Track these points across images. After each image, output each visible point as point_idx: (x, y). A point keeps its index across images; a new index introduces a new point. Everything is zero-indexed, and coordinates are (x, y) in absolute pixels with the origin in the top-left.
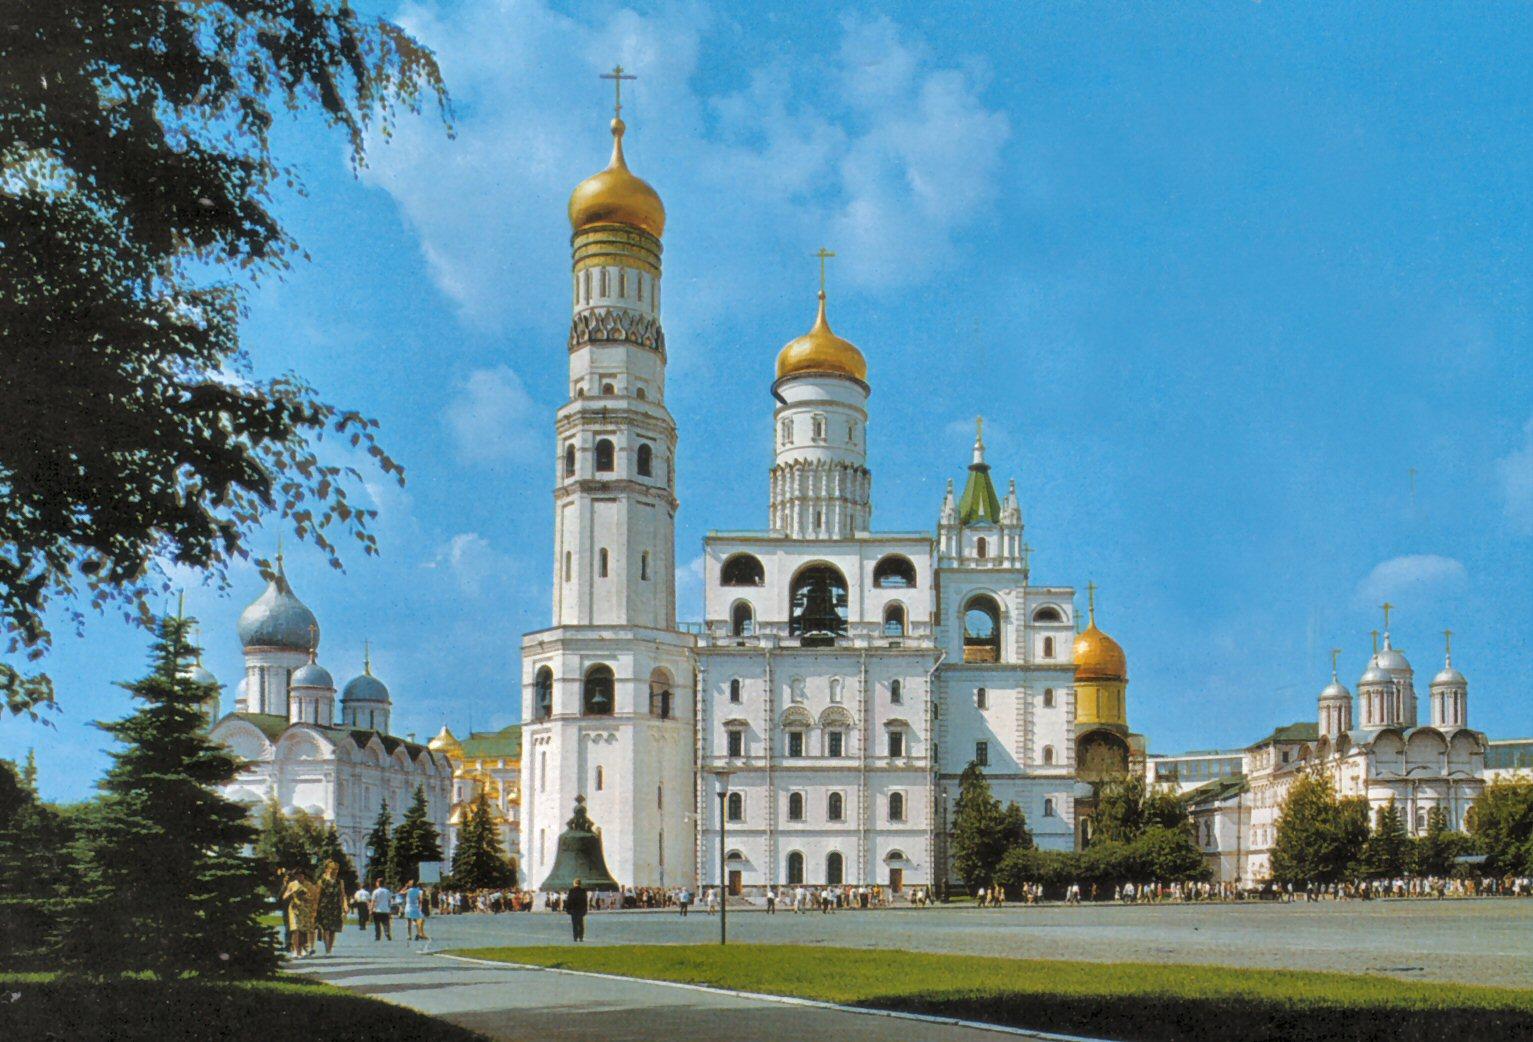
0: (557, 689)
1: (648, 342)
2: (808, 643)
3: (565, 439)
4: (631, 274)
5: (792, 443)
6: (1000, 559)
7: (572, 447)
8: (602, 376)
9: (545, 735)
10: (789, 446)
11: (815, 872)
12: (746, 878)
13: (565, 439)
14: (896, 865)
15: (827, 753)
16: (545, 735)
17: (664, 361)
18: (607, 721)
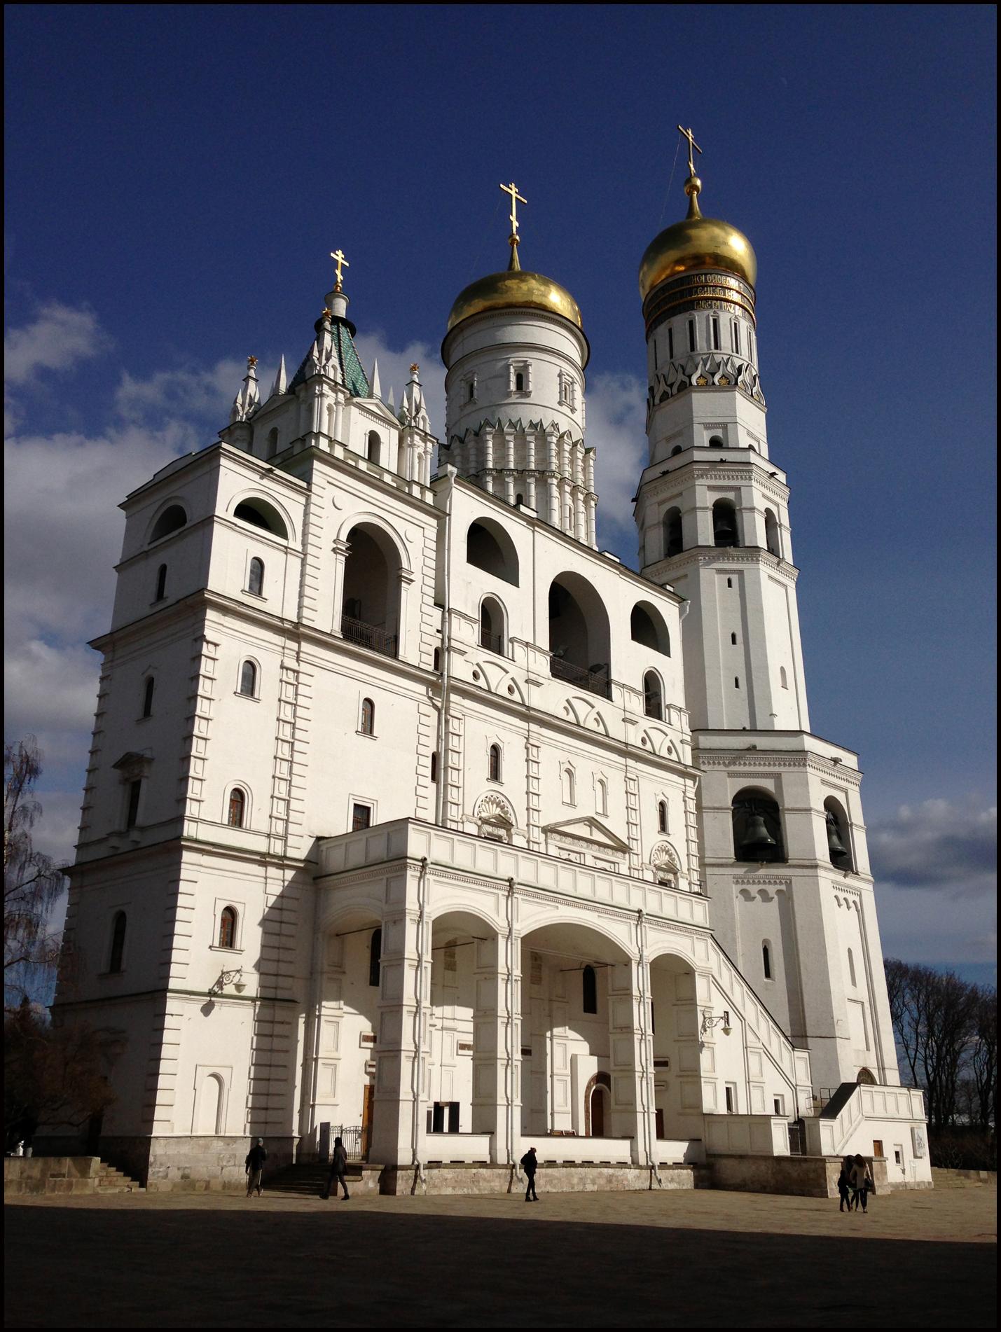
8: (708, 426)
13: (660, 503)
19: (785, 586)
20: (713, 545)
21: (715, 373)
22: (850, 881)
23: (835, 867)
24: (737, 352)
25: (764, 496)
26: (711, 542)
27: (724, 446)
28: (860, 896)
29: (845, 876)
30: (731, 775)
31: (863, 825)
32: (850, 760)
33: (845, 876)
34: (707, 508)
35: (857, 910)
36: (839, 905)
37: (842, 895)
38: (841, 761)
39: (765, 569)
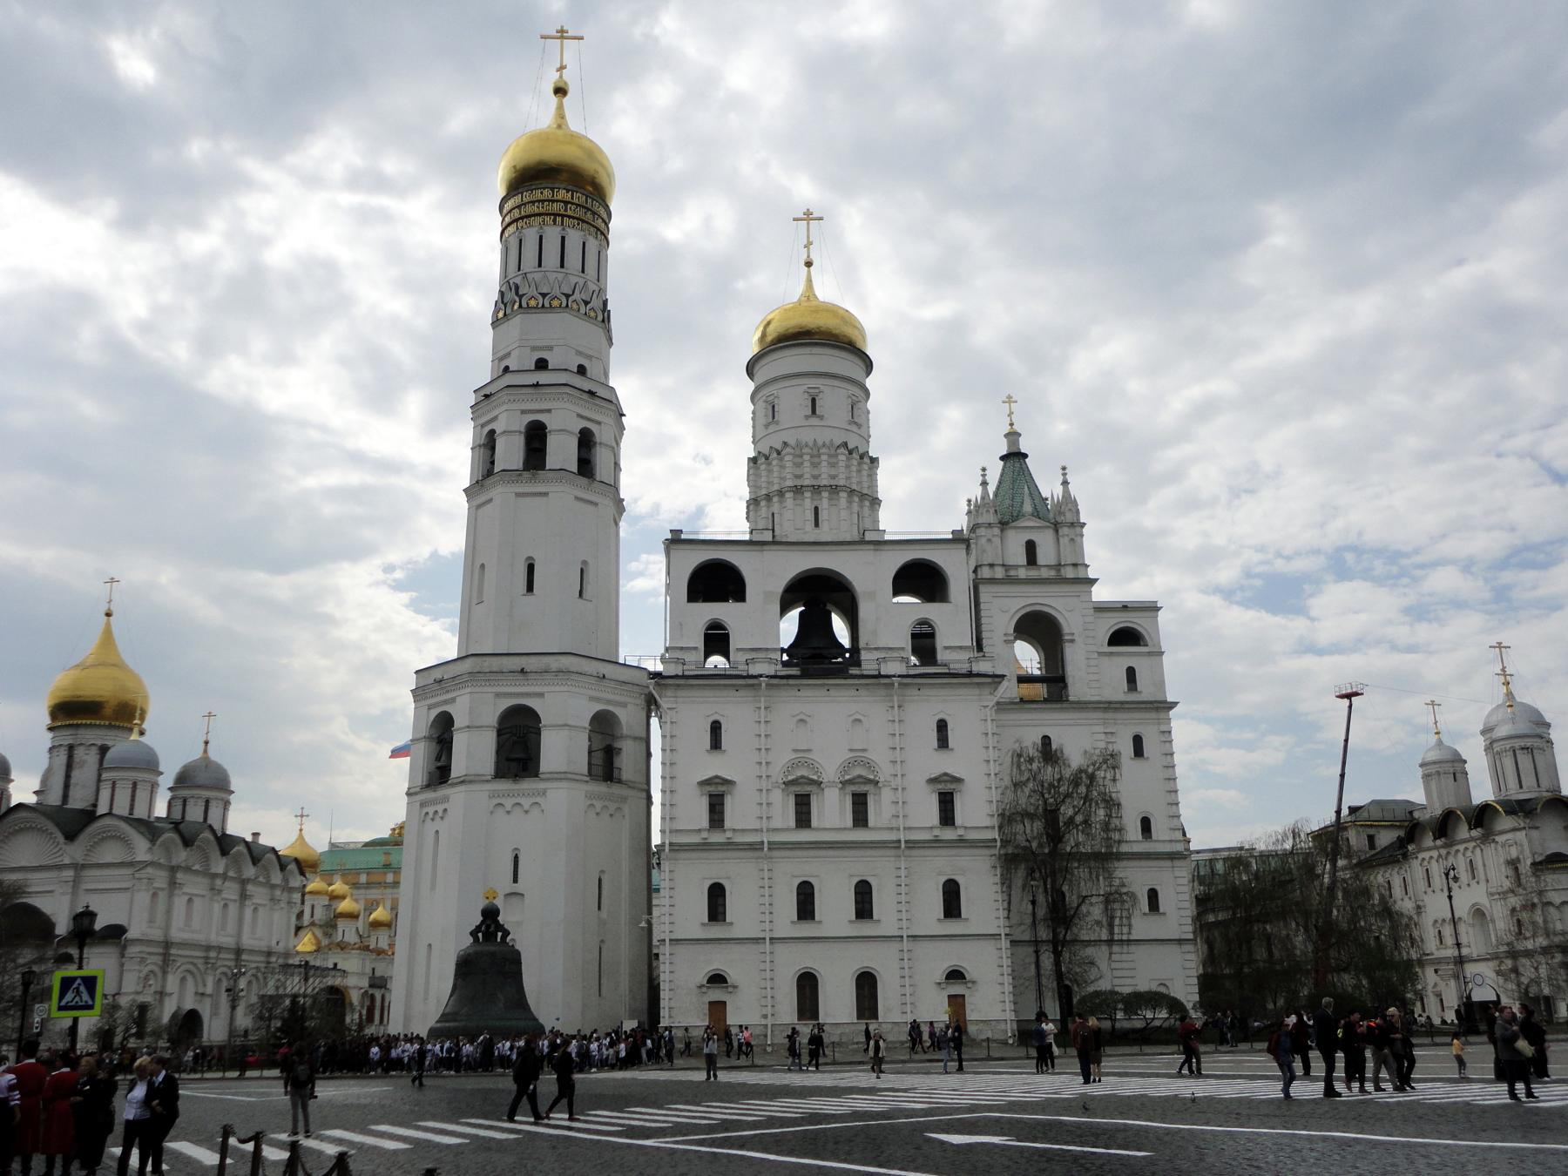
0: (460, 742)
1: (592, 314)
2: (804, 675)
3: (483, 426)
4: (574, 237)
5: (777, 423)
6: (1058, 566)
7: (492, 432)
8: (534, 349)
10: (772, 428)
11: (838, 1006)
12: (733, 1019)
13: (483, 426)
14: (957, 989)
15: (850, 823)
16: (440, 808)
17: (610, 342)
18: (527, 784)
21: (548, 294)
27: (550, 368)
30: (498, 695)
34: (520, 432)
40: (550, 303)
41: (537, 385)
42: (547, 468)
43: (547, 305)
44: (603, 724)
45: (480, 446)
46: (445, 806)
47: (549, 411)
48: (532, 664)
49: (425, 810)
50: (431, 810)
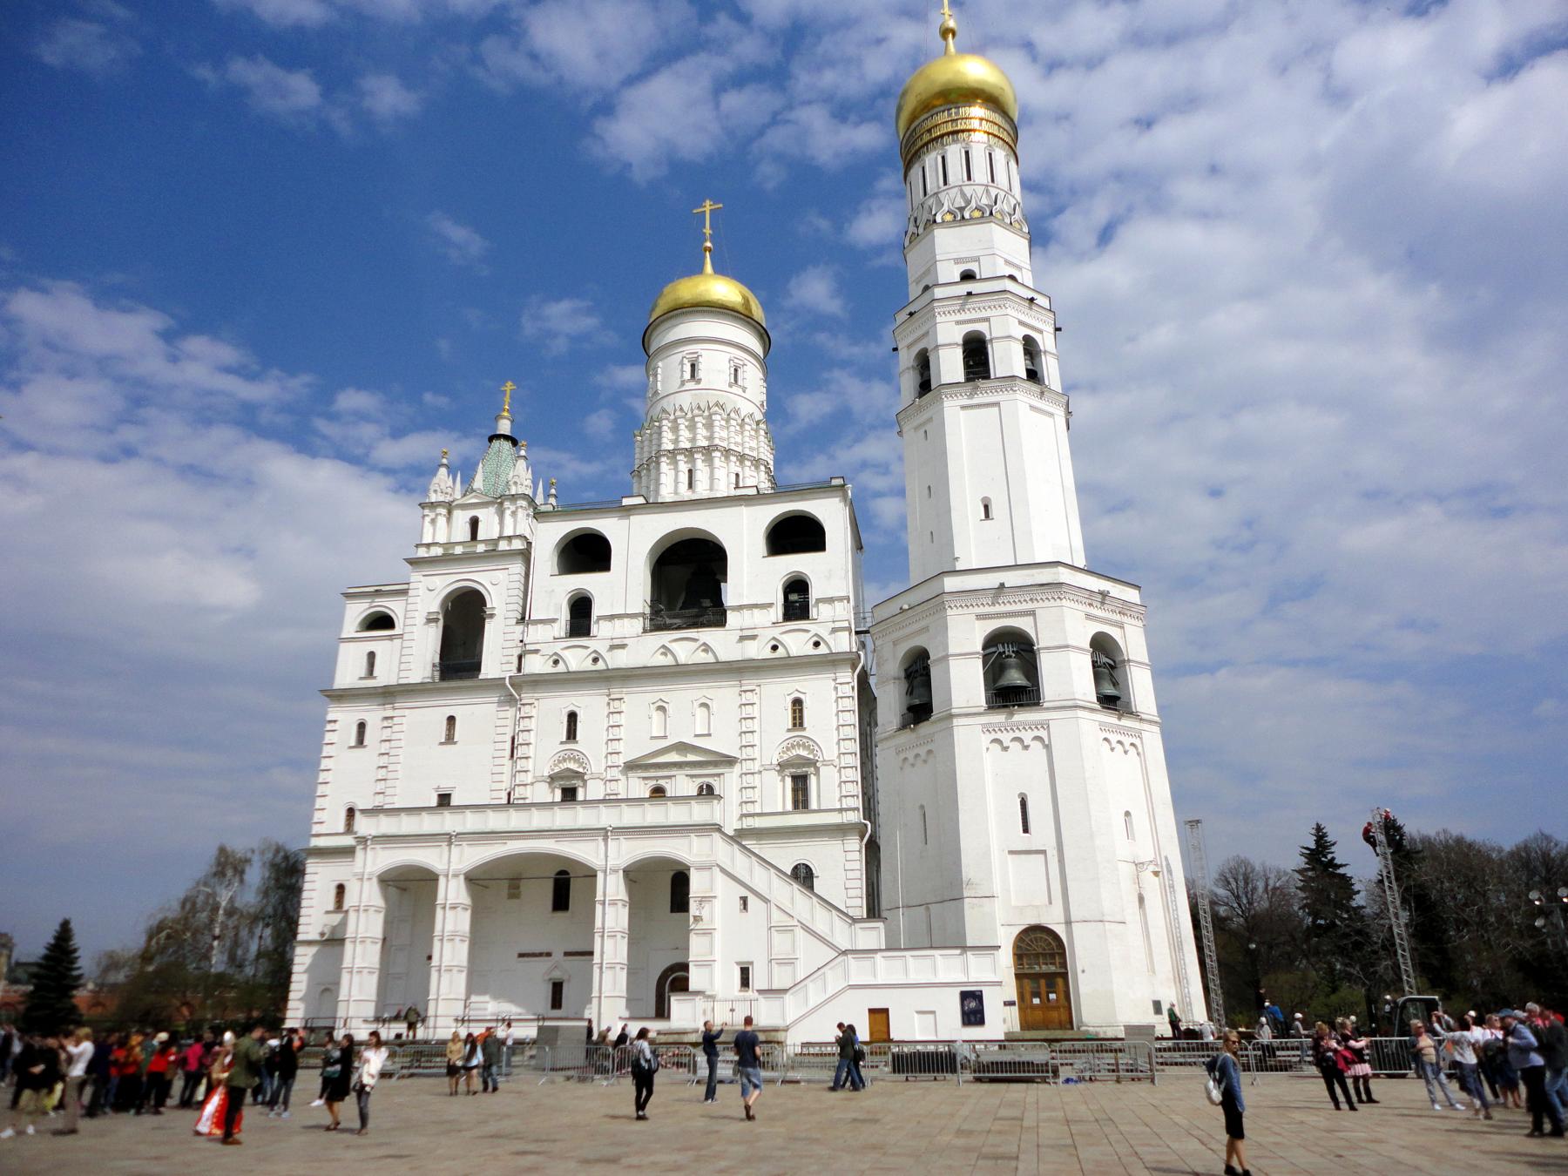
8: (958, 261)
9: (922, 751)
16: (922, 751)
19: (1051, 415)
20: (962, 379)
21: (966, 207)
22: (1126, 722)
23: (1104, 708)
24: (993, 181)
25: (1021, 323)
26: (961, 377)
27: (978, 277)
28: (1141, 739)
29: (1119, 719)
30: (980, 617)
31: (1147, 661)
32: (1132, 595)
33: (1119, 719)
35: (1138, 754)
36: (1112, 749)
37: (1114, 738)
38: (1108, 592)
39: (1022, 399)
40: (970, 215)
41: (969, 294)
42: (992, 377)
43: (967, 216)
44: (1102, 647)
45: (908, 368)
46: (929, 747)
47: (987, 320)
48: (1011, 579)
49: (902, 756)
50: (910, 755)
